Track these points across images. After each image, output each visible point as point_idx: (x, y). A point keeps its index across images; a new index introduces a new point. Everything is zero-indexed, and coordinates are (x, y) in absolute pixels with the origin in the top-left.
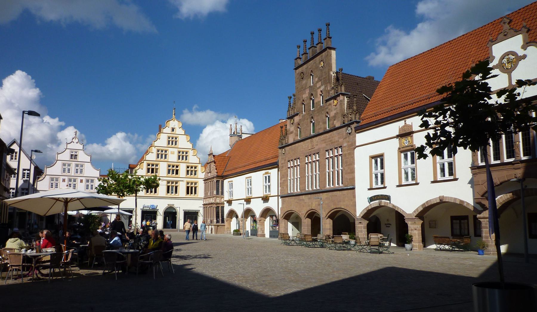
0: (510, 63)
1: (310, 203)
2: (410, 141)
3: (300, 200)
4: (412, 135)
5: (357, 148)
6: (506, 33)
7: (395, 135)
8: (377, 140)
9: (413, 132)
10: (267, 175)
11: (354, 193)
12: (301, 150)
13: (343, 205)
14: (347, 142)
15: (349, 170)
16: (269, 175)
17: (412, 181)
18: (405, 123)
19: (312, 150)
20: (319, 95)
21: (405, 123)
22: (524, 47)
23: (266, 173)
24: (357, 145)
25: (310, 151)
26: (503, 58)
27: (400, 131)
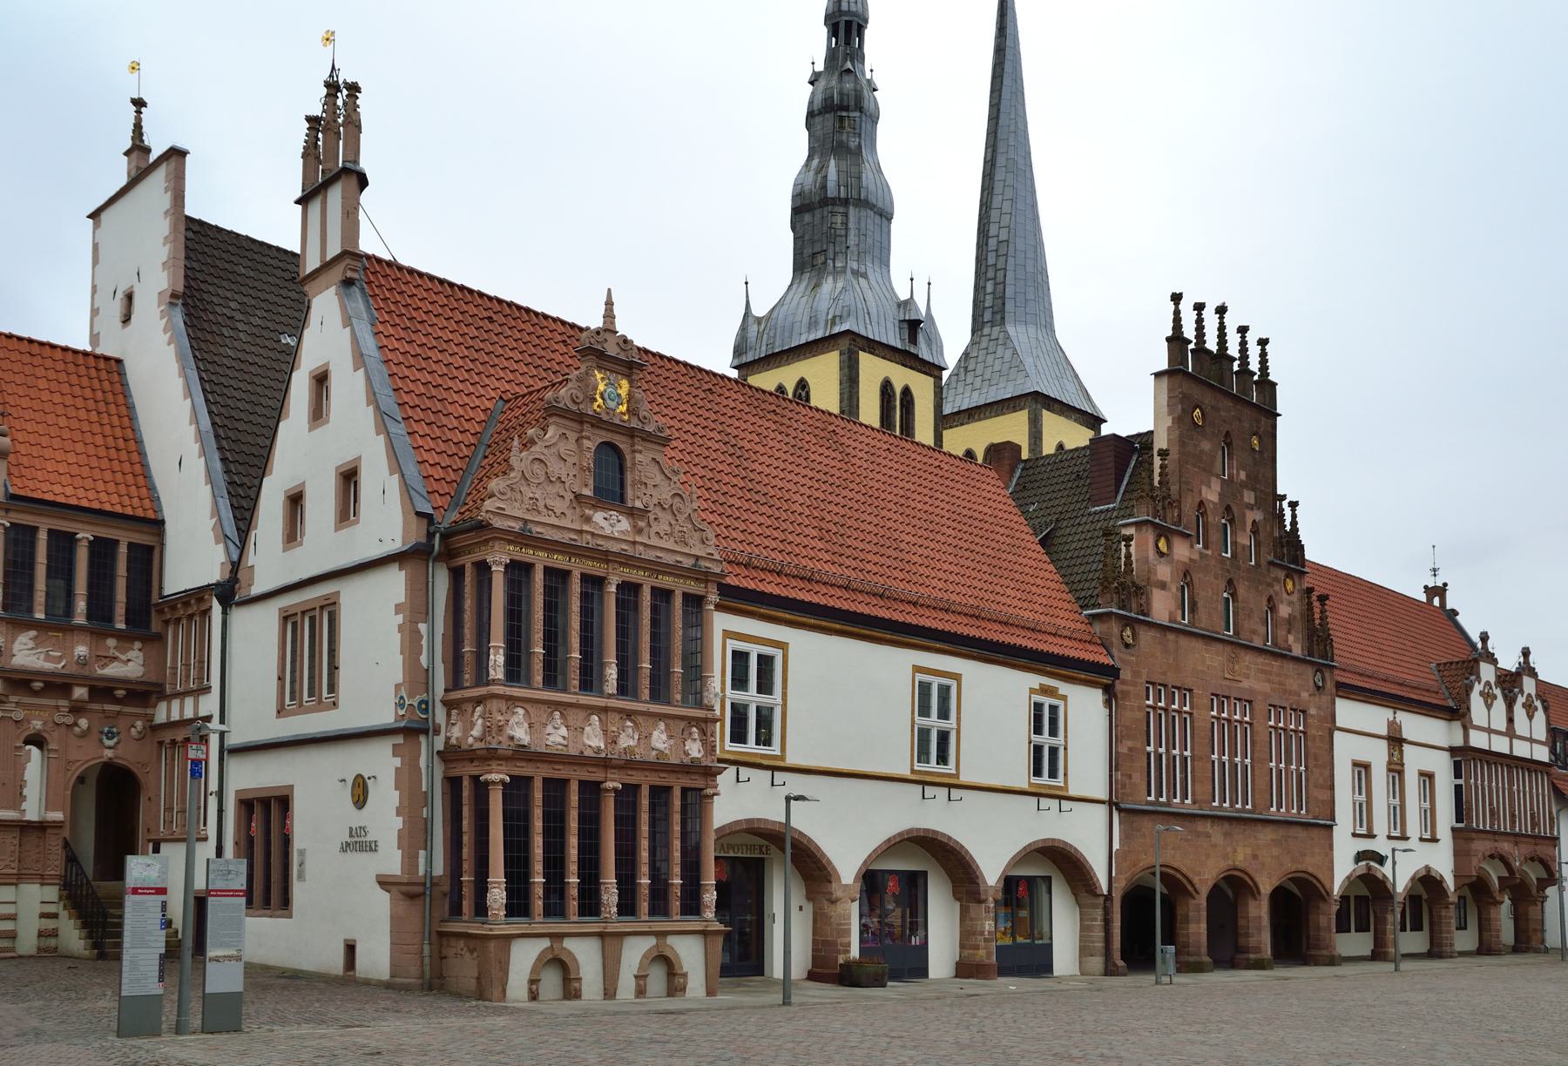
1: (1229, 849)
3: (1198, 834)
9: (1405, 741)
10: (1047, 701)
11: (1331, 837)
12: (1200, 668)
13: (1310, 864)
16: (1055, 702)
23: (1045, 690)
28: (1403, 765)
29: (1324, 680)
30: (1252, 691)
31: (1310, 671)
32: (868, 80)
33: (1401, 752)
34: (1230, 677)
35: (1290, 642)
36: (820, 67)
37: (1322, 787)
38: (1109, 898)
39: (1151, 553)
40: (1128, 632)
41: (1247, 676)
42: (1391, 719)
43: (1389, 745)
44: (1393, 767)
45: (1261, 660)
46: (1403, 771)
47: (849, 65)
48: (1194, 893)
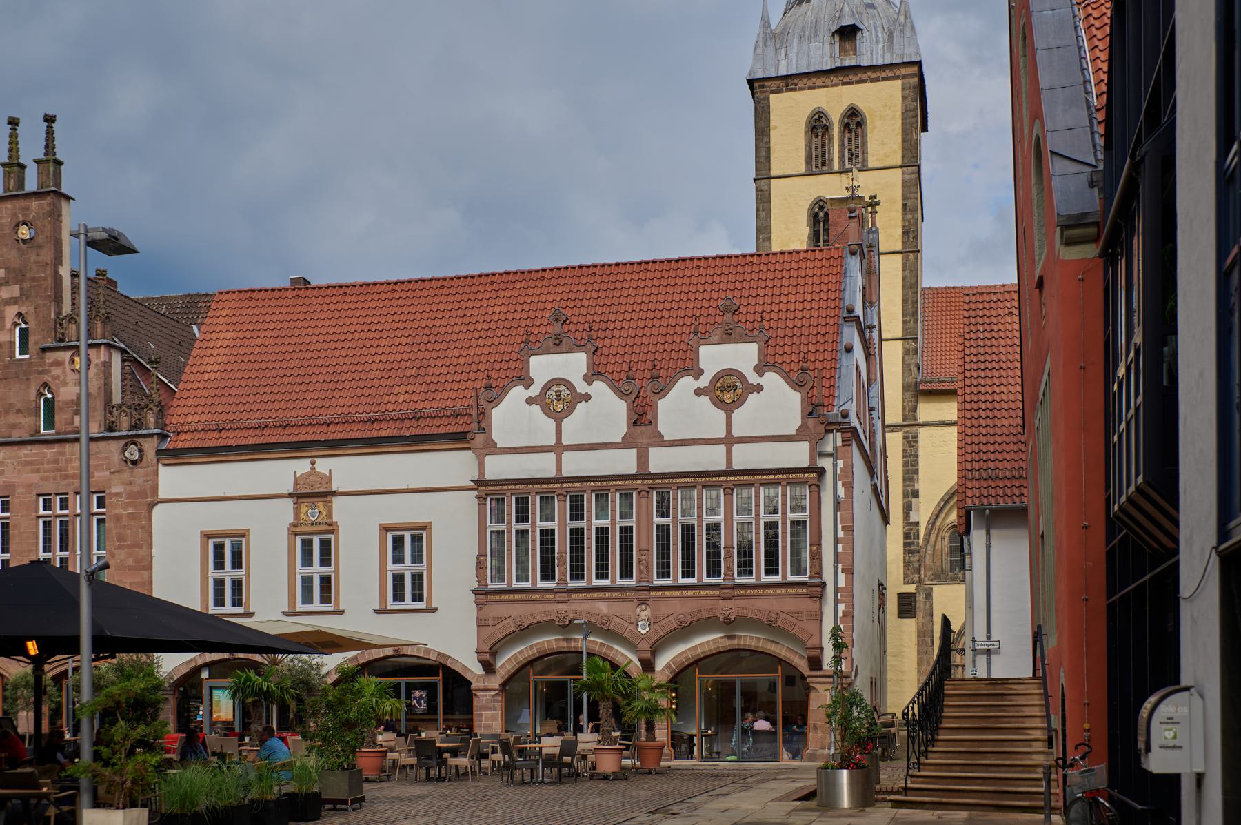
0: (561, 402)
2: (322, 511)
4: (329, 499)
5: (160, 505)
6: (558, 342)
7: (285, 492)
9: (334, 494)
14: (123, 483)
15: (131, 560)
17: (321, 603)
20: (8, 325)
22: (588, 379)
24: (161, 496)
26: (547, 387)
27: (296, 483)
31: (115, 446)
45: (26, 451)
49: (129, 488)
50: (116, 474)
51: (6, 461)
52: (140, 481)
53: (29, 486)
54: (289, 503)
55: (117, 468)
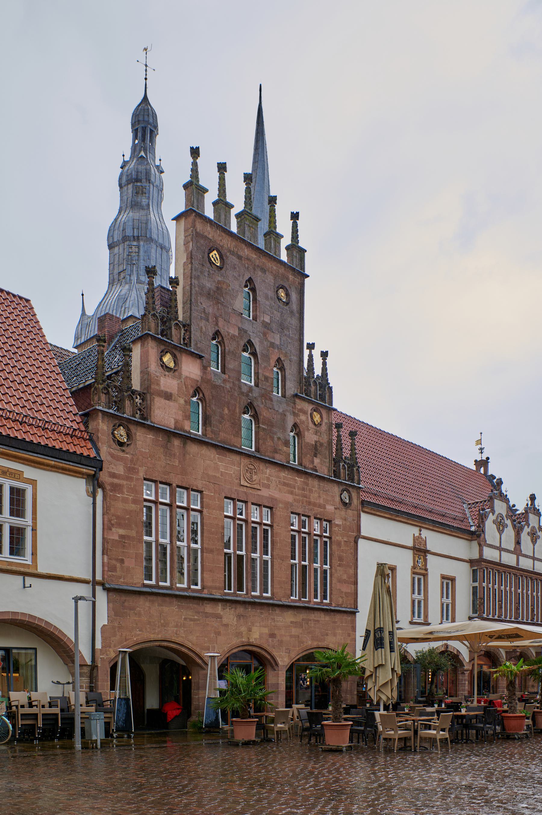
8: (390, 541)
9: (428, 552)
14: (341, 518)
18: (420, 534)
19: (251, 491)
21: (420, 534)
25: (245, 493)
28: (426, 570)
29: (350, 498)
30: (273, 499)
31: (336, 490)
32: (157, 166)
33: (425, 560)
34: (246, 484)
35: (315, 464)
36: (127, 158)
37: (345, 582)
38: (94, 667)
39: (154, 367)
40: (122, 431)
41: (268, 487)
42: (417, 534)
43: (414, 554)
44: (415, 571)
45: (284, 474)
46: (427, 574)
47: (142, 154)
48: (203, 665)
49: (344, 522)
50: (338, 510)
51: (271, 478)
52: (350, 519)
53: (287, 505)
54: (410, 553)
55: (338, 506)
